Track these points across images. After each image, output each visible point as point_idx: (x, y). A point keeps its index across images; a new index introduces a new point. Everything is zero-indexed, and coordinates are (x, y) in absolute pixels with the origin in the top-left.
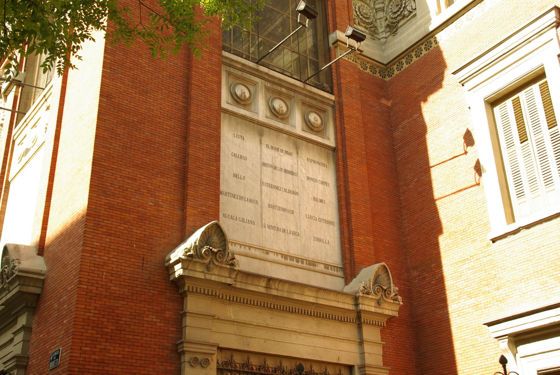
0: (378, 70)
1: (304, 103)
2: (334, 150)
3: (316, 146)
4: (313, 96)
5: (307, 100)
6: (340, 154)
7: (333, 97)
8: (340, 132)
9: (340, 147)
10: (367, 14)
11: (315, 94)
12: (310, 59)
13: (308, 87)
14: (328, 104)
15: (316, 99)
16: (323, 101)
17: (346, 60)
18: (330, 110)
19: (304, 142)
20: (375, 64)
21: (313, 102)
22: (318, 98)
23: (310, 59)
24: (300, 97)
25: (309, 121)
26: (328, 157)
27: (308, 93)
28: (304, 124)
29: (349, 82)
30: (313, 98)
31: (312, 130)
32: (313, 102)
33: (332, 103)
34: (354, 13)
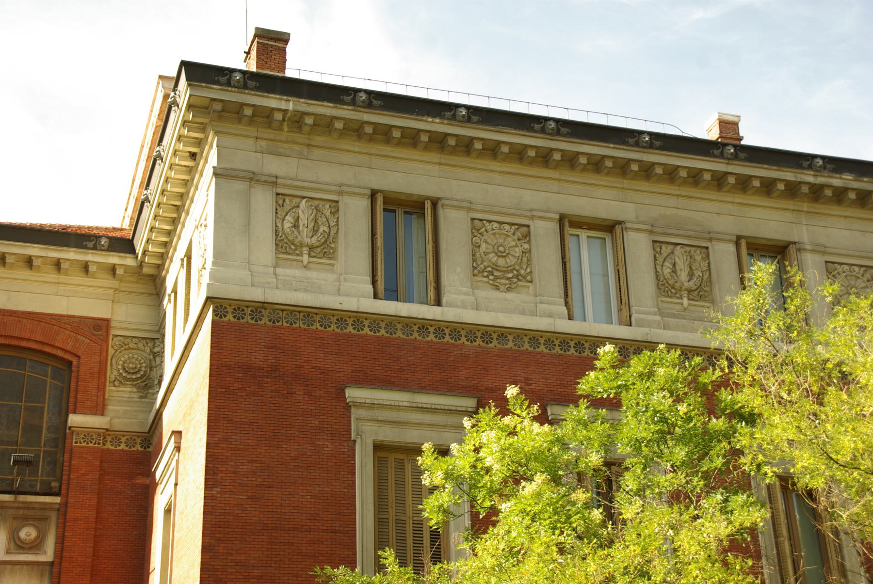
0: (139, 441)
1: (15, 518)
2: (52, 564)
3: (25, 567)
4: (28, 506)
5: (21, 512)
6: (56, 569)
7: (57, 500)
8: (61, 541)
9: (58, 560)
10: (135, 368)
11: (31, 503)
12: (45, 452)
13: (22, 498)
14: (52, 509)
15: (34, 508)
16: (44, 507)
17: (83, 447)
18: (54, 516)
19: (9, 567)
20: (132, 436)
21: (30, 513)
22: (36, 506)
23: (45, 452)
24: (10, 512)
25: (19, 538)
26: (42, 575)
27: (21, 505)
28: (12, 545)
29: (82, 475)
30: (28, 508)
31: (23, 548)
32: (30, 513)
33: (57, 507)
34: (115, 373)
